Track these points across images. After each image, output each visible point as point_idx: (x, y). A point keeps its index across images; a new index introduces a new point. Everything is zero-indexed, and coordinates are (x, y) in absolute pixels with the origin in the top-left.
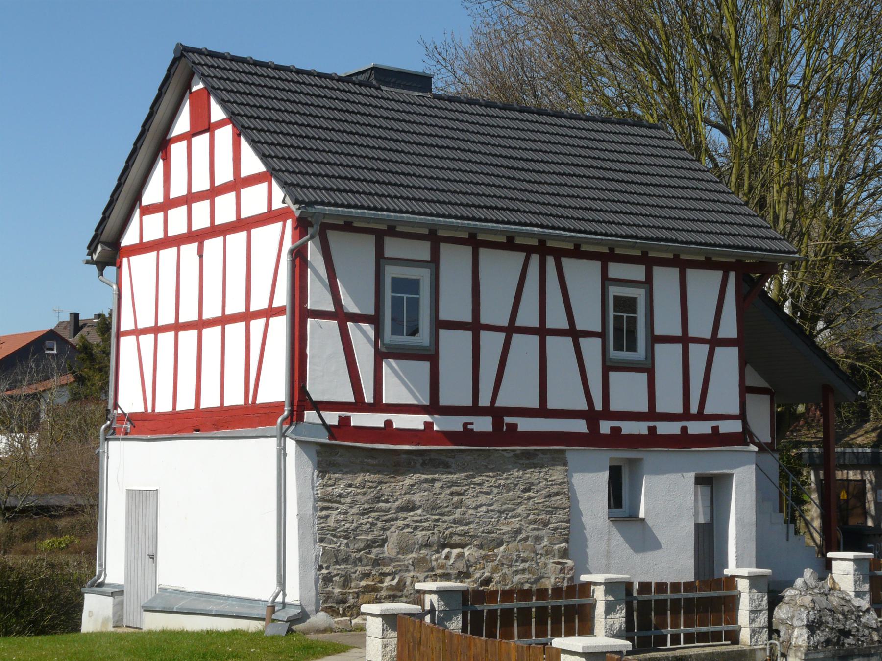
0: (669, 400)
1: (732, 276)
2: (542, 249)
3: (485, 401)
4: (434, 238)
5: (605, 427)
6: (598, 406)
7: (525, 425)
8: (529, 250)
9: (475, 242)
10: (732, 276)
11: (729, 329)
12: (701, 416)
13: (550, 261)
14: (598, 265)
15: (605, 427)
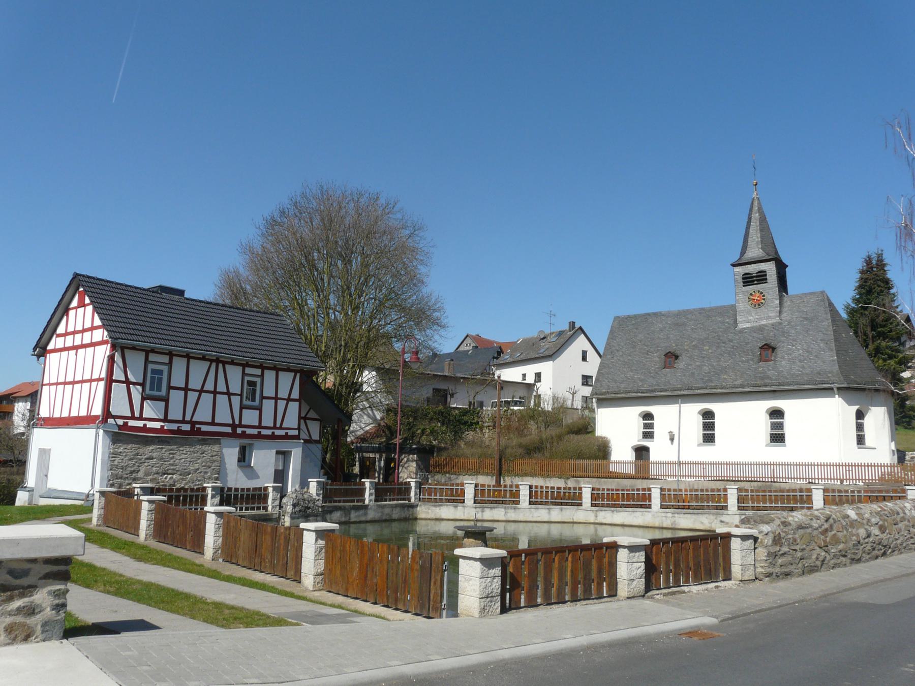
0: (268, 421)
1: (298, 375)
2: (217, 361)
3: (188, 418)
4: (171, 355)
5: (239, 430)
6: (237, 422)
7: (204, 428)
8: (211, 361)
9: (188, 357)
10: (298, 375)
11: (296, 394)
12: (281, 428)
13: (221, 366)
14: (241, 368)
15: (239, 430)
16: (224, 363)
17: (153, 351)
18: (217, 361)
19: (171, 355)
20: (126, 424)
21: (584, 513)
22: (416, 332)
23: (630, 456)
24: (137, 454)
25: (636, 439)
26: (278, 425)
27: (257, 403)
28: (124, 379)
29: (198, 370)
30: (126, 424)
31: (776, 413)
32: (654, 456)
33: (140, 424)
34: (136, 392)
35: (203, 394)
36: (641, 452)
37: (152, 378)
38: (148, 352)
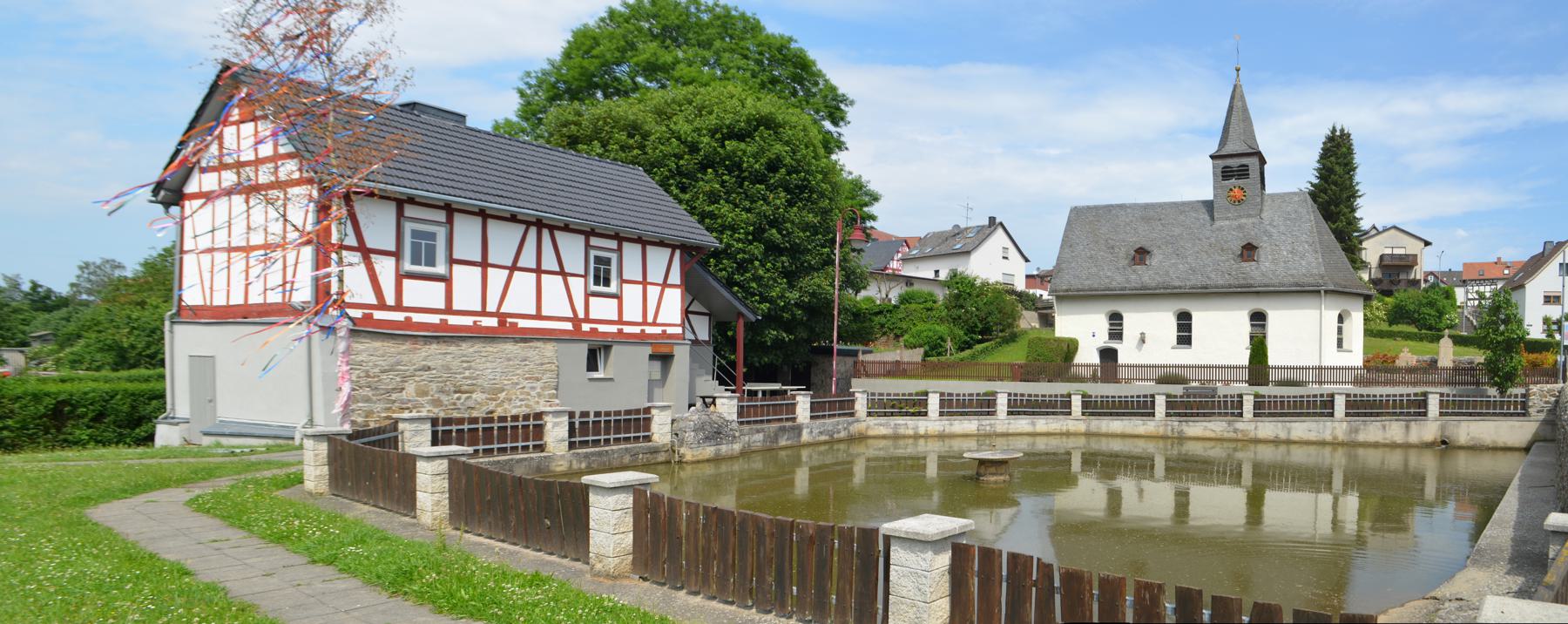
0: (632, 312)
1: (678, 253)
2: (540, 224)
3: (491, 307)
4: (450, 210)
5: (586, 327)
6: (581, 315)
7: (522, 323)
8: (528, 224)
9: (483, 215)
10: (678, 253)
11: (675, 277)
12: (654, 324)
13: (546, 233)
14: (582, 238)
15: (586, 327)
16: (552, 228)
17: (412, 200)
18: (540, 224)
19: (450, 210)
20: (368, 317)
21: (1076, 422)
22: (240, 49)
23: (1096, 360)
24: (398, 364)
25: (1103, 340)
26: (650, 320)
27: (613, 288)
28: (557, 269)
29: (504, 240)
30: (368, 317)
31: (1258, 318)
32: (1122, 359)
33: (399, 316)
34: (577, 285)
35: (516, 273)
36: (1108, 355)
37: (597, 270)
38: (401, 203)
